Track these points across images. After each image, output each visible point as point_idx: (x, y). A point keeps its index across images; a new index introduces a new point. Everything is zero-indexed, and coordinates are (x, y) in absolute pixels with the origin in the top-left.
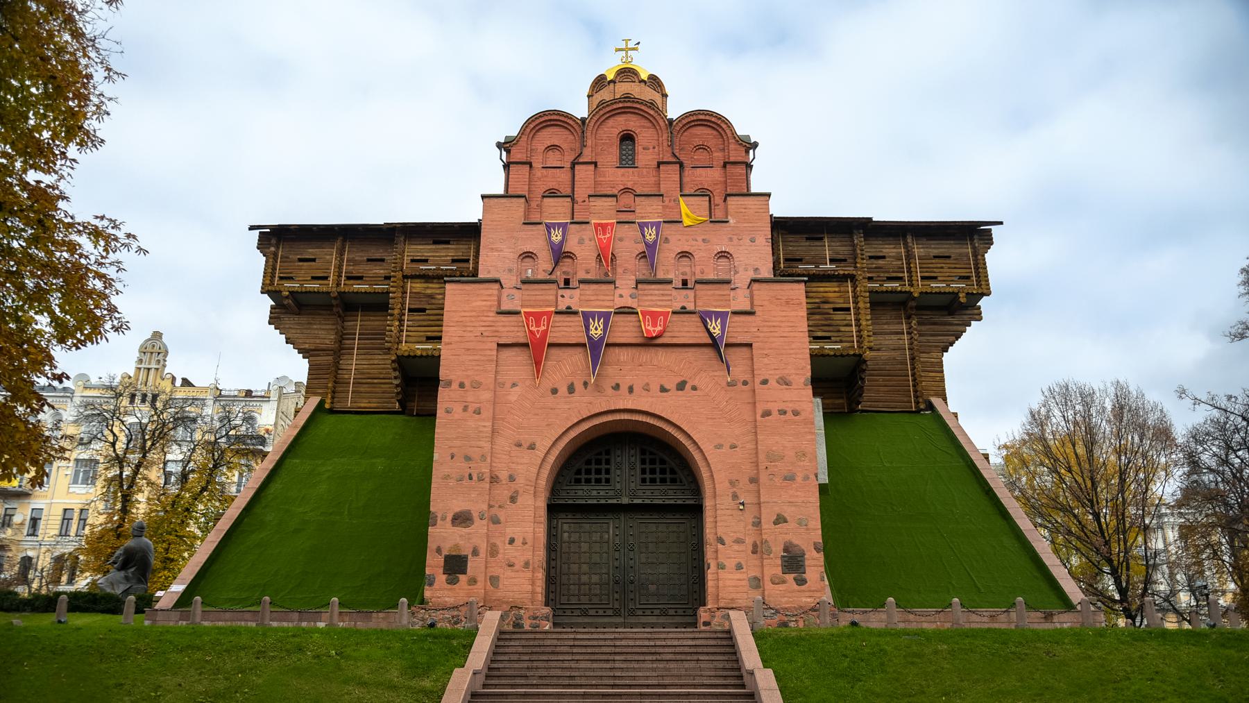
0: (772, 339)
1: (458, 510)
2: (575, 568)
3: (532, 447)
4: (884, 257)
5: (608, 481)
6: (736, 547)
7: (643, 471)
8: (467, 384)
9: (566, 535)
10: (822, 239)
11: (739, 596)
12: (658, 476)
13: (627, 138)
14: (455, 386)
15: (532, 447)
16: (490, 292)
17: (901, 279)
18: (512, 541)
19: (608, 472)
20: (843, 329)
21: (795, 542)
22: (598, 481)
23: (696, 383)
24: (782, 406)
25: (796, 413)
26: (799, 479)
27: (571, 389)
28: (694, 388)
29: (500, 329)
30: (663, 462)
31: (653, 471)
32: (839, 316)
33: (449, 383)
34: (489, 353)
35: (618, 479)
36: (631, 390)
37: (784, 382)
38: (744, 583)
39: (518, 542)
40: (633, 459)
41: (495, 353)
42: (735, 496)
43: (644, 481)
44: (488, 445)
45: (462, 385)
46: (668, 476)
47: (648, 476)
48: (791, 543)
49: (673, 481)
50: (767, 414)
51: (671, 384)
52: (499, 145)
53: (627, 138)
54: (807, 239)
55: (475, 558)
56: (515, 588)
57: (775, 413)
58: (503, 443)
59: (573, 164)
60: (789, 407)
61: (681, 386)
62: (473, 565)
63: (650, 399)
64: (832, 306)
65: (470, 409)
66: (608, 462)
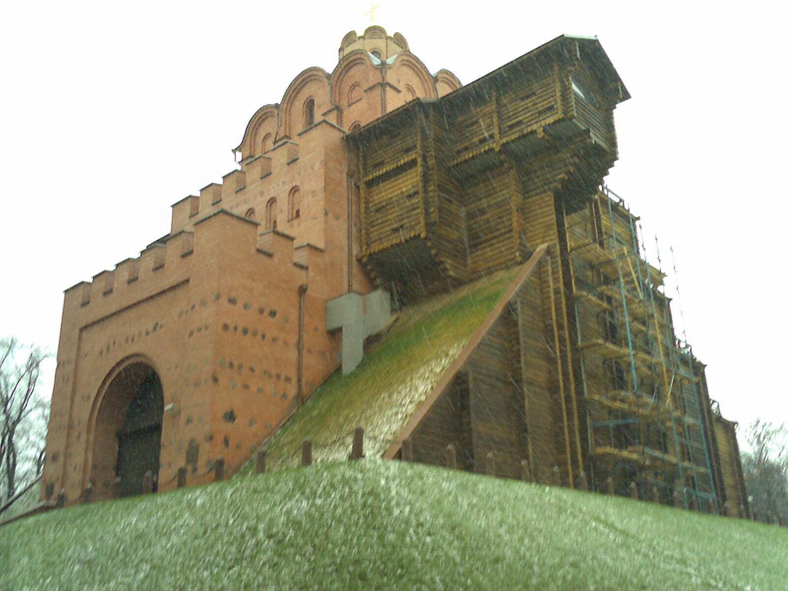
27: (108, 349)
44: (68, 402)
50: (191, 334)
51: (151, 329)
52: (234, 151)
58: (78, 398)
61: (155, 328)
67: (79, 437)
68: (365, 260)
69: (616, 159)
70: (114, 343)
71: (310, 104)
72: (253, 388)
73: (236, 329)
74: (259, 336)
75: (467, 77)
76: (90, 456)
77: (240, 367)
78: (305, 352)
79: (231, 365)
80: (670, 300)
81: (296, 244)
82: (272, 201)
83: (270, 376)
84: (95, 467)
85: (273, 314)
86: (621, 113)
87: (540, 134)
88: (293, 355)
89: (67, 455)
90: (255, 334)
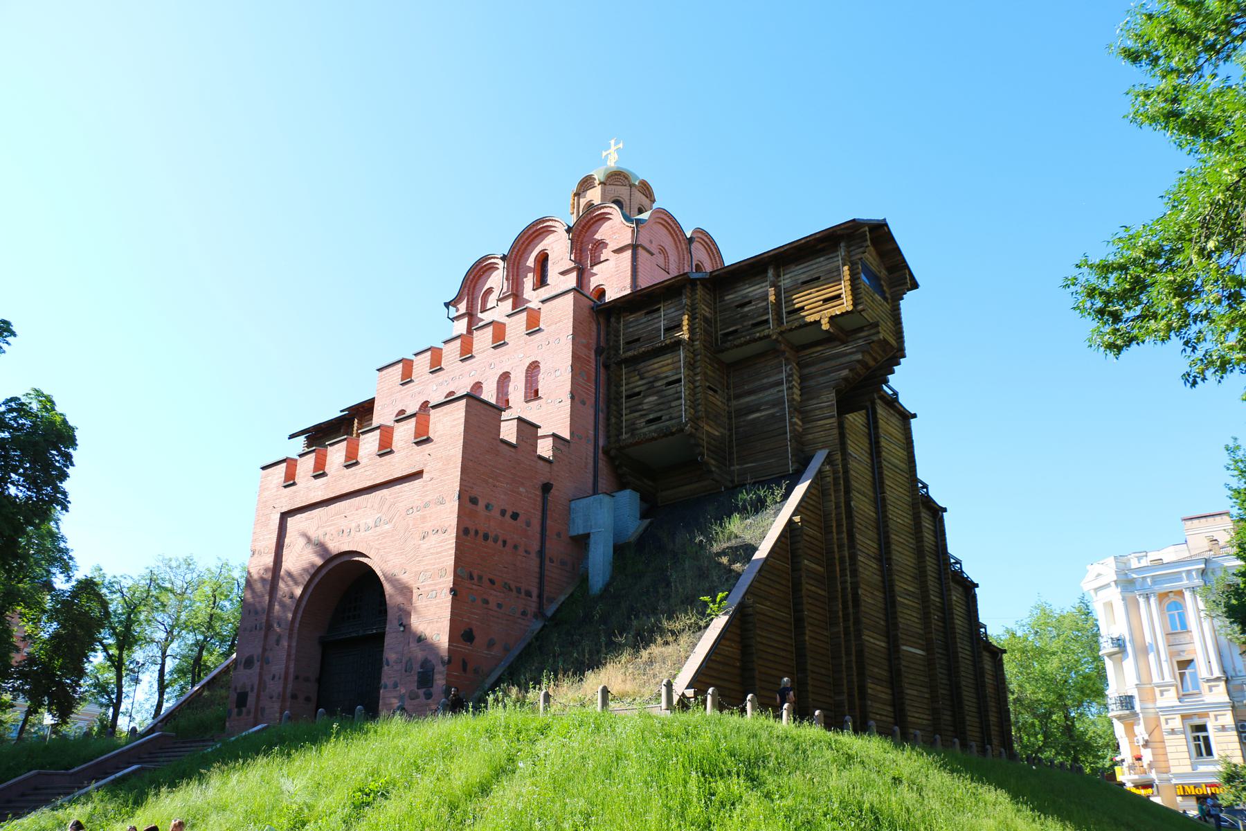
4: (750, 302)
10: (659, 309)
17: (767, 321)
18: (274, 677)
20: (673, 404)
21: (430, 658)
32: (671, 390)
51: (371, 524)
52: (447, 305)
54: (647, 313)
62: (251, 699)
64: (665, 382)
67: (278, 642)
68: (613, 453)
69: (904, 356)
71: (543, 259)
72: (492, 605)
73: (477, 532)
74: (500, 542)
75: (736, 250)
76: (292, 666)
77: (480, 578)
78: (547, 562)
79: (471, 578)
80: (945, 510)
81: (540, 432)
82: (505, 377)
83: (511, 590)
84: (297, 678)
85: (515, 516)
86: (909, 304)
87: (825, 326)
88: (534, 563)
89: (265, 661)
90: (495, 541)
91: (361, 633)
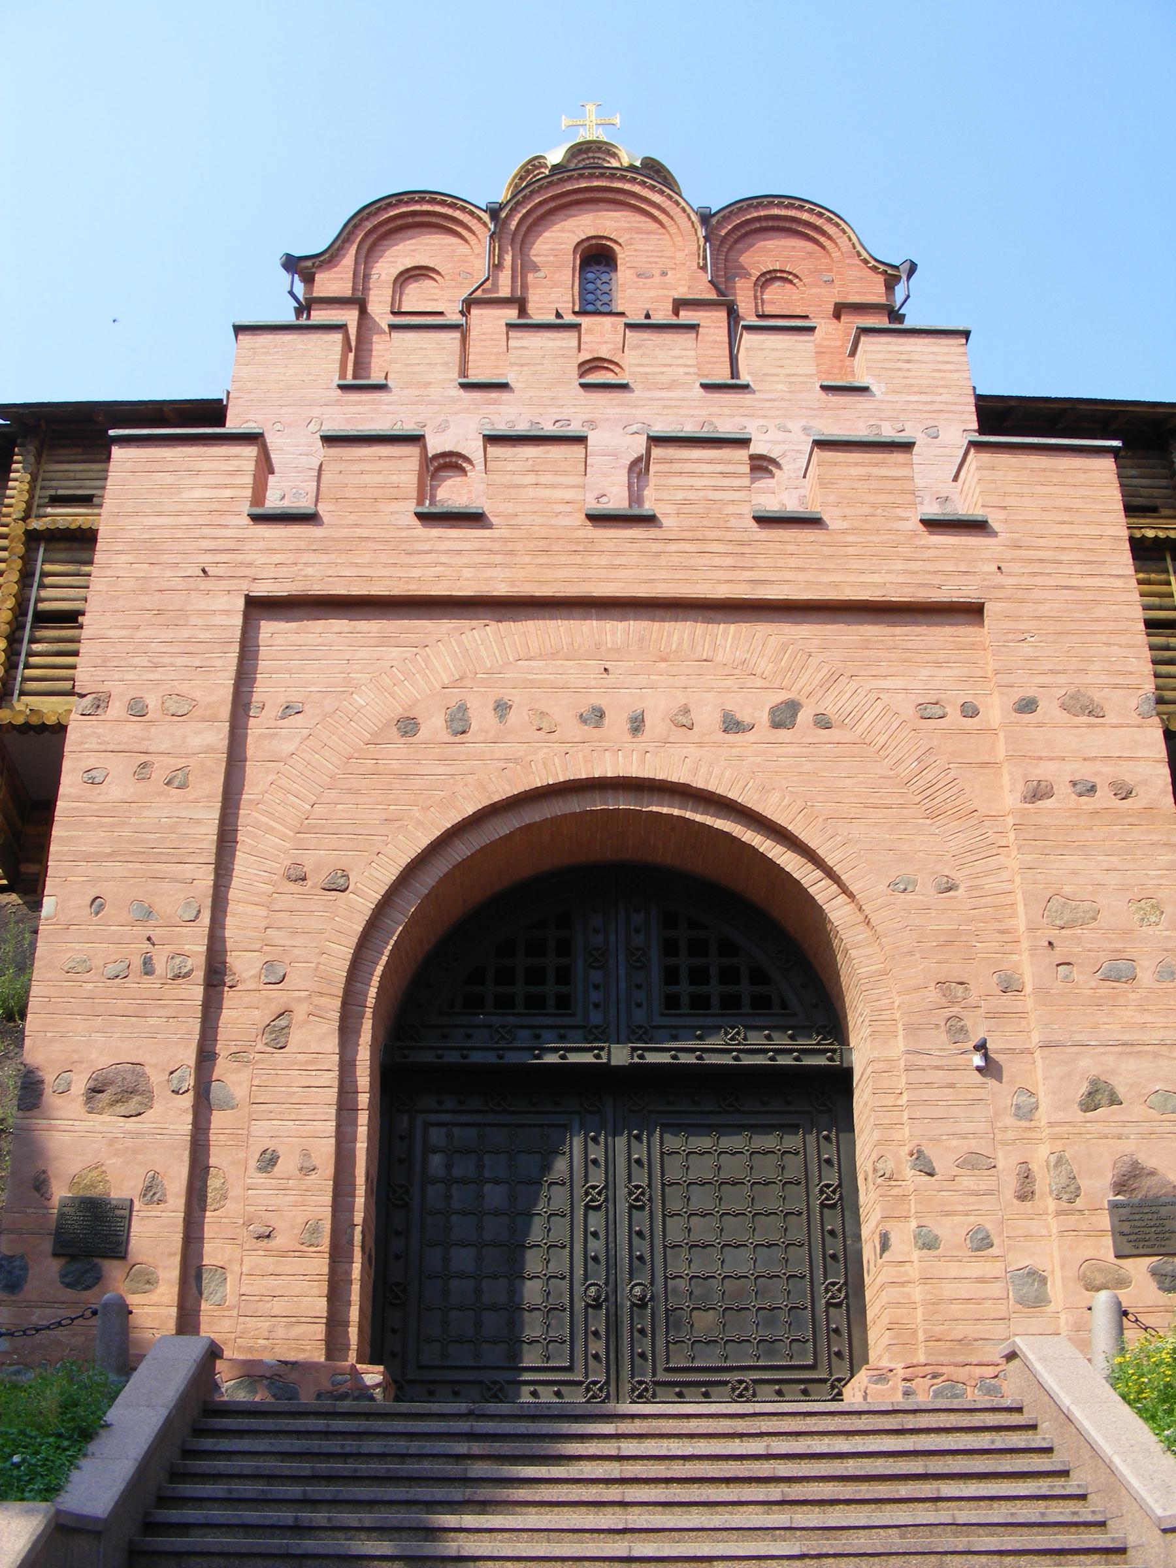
0: (1037, 594)
1: (102, 1060)
2: (464, 1259)
3: (338, 886)
5: (564, 1003)
6: (968, 1181)
7: (671, 976)
8: (152, 701)
9: (436, 1160)
11: (982, 1329)
12: (714, 989)
13: (597, 258)
14: (116, 709)
15: (338, 886)
16: (234, 464)
18: (269, 1161)
19: (564, 976)
21: (1149, 1160)
22: (536, 1004)
23: (829, 706)
24: (1085, 772)
25: (1125, 793)
26: (1146, 976)
28: (823, 722)
29: (261, 559)
30: (728, 948)
31: (699, 976)
33: (101, 703)
34: (219, 620)
35: (595, 996)
36: (637, 725)
37: (1084, 707)
38: (996, 1289)
39: (287, 1165)
40: (639, 940)
41: (238, 620)
42: (956, 1029)
43: (672, 1003)
45: (137, 709)
46: (745, 989)
47: (684, 989)
48: (1135, 1165)
49: (761, 1003)
50: (1038, 793)
52: (291, 264)
53: (597, 258)
55: (155, 1210)
56: (278, 1306)
57: (1063, 790)
59: (469, 304)
60: (1102, 773)
61: (784, 716)
63: (693, 751)
65: (159, 775)
66: (564, 949)
67: (277, 1032)
70: (502, 708)
91: (620, 1055)
